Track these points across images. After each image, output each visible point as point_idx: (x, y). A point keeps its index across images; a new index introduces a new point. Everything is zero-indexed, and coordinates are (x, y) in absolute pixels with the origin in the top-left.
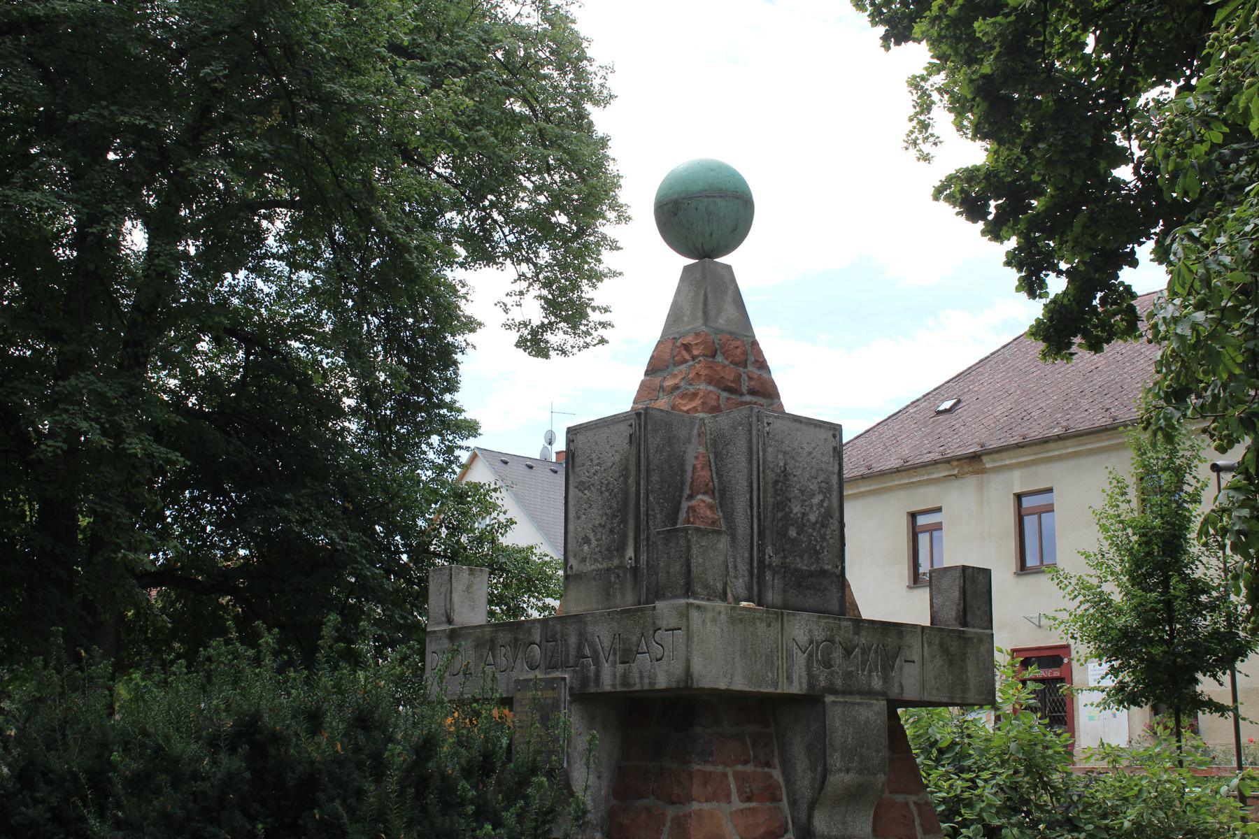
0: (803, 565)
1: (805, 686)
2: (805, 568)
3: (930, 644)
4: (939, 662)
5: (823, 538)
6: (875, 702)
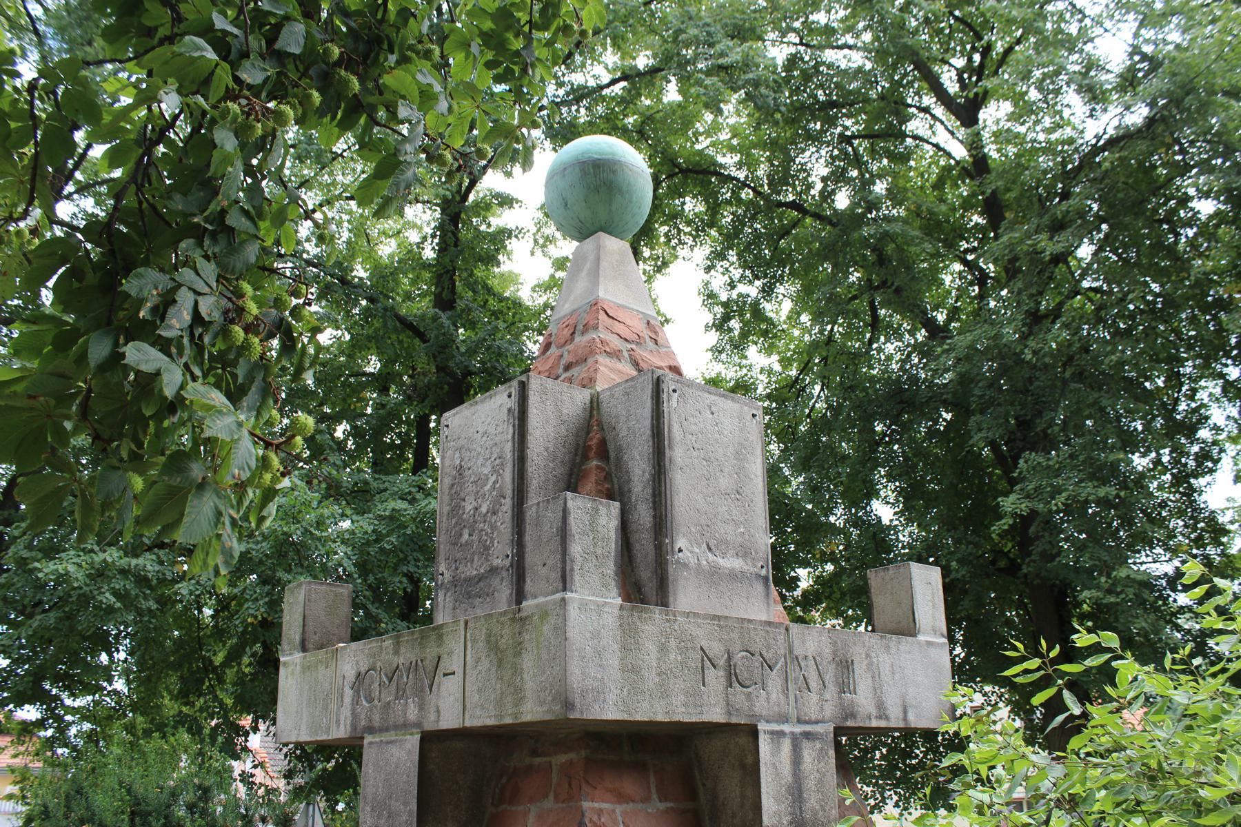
0: (470, 571)
1: (349, 728)
2: (475, 573)
3: (474, 641)
4: (485, 665)
5: (494, 527)
6: (408, 737)
